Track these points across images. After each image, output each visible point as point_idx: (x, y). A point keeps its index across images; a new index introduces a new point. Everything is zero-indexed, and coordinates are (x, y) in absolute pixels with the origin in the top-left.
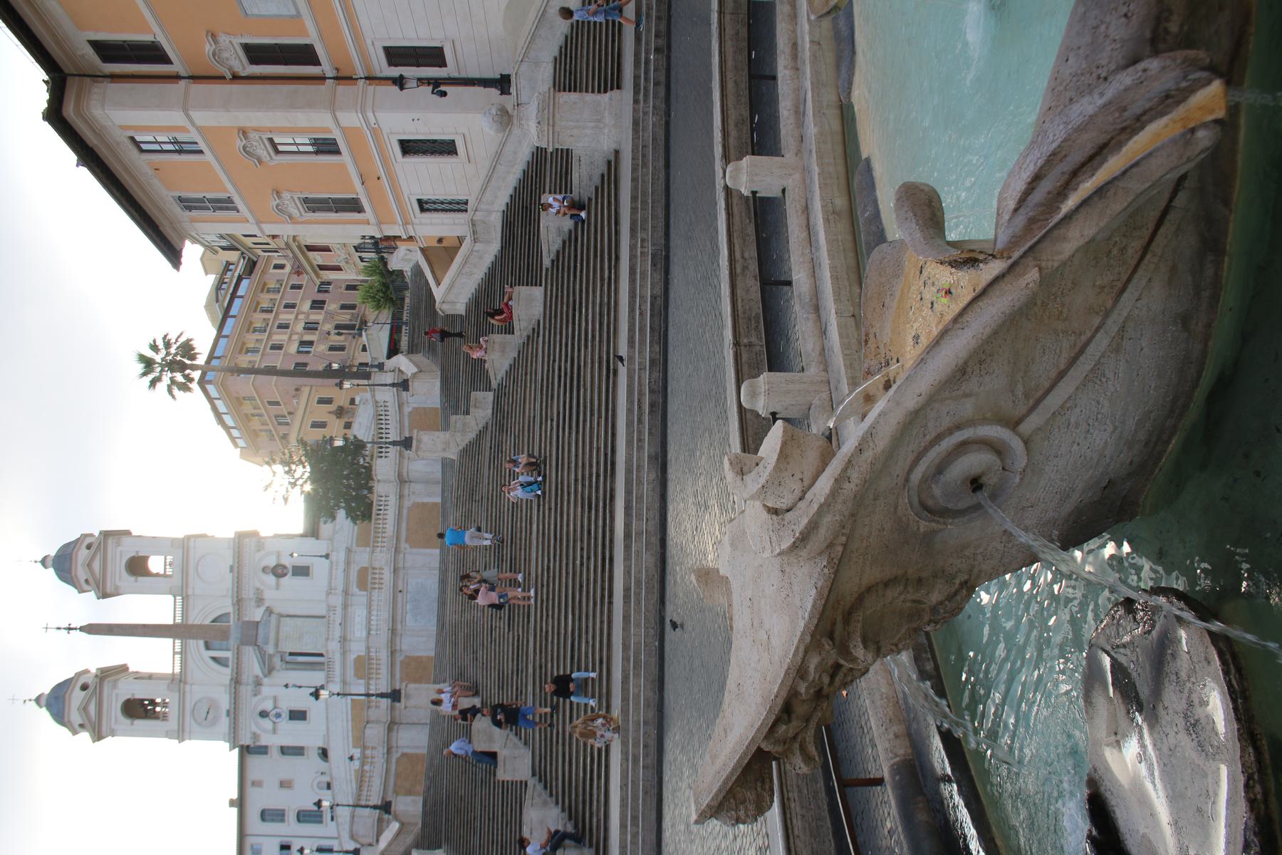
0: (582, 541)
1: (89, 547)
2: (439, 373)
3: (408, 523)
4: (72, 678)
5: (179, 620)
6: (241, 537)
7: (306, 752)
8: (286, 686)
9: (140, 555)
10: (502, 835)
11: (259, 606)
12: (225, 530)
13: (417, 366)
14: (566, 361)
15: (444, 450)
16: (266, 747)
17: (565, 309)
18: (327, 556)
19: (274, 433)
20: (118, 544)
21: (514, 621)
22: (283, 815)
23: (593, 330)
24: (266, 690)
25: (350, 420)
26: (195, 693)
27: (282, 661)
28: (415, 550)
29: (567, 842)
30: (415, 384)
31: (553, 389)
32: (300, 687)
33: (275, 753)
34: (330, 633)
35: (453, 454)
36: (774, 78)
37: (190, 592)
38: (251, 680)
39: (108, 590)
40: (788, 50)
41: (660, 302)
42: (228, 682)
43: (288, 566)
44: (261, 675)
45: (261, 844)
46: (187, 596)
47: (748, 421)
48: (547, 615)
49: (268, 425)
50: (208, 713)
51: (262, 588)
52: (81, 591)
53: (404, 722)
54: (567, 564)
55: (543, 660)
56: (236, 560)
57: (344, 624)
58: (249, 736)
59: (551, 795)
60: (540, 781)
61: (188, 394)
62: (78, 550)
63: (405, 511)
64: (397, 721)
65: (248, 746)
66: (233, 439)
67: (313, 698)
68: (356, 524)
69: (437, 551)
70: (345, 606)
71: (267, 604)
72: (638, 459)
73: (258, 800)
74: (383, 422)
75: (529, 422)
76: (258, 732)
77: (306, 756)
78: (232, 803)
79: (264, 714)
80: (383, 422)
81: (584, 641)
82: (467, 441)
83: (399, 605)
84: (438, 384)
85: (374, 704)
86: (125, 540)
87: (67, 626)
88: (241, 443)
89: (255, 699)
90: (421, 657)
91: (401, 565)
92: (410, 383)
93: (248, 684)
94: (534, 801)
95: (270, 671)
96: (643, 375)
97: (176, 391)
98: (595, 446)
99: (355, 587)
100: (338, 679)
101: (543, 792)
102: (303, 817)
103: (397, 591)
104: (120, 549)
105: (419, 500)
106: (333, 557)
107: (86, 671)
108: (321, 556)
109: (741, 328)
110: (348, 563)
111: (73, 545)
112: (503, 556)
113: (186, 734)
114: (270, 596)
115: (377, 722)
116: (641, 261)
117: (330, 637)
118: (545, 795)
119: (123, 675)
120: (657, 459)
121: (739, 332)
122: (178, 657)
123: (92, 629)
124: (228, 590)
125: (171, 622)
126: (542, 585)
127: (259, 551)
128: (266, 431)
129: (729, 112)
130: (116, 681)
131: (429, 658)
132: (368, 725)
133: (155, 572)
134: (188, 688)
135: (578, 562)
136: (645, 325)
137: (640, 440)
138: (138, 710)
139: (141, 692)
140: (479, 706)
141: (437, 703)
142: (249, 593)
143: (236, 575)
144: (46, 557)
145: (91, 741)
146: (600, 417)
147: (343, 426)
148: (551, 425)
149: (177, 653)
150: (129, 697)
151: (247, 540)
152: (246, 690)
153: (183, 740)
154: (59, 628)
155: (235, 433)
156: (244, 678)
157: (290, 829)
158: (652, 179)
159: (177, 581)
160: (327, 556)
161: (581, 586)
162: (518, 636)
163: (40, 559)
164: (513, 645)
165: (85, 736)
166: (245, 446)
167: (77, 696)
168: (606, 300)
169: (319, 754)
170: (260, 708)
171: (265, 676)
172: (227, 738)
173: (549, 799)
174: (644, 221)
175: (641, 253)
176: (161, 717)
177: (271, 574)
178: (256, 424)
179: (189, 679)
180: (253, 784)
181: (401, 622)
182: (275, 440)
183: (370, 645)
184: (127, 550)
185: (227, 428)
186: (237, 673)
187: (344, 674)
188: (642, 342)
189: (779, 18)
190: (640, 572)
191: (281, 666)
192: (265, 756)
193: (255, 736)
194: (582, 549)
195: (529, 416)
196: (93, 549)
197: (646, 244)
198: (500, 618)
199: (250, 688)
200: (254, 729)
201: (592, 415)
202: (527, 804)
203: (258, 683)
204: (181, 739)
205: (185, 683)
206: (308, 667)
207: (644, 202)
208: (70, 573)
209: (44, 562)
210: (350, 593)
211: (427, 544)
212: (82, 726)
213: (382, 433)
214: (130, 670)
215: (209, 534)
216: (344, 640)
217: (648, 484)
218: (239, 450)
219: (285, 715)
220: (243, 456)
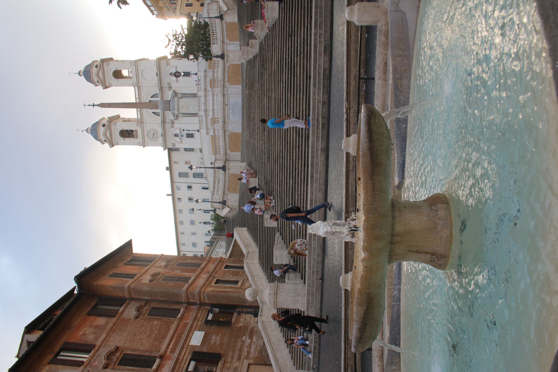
0: (296, 149)
1: (96, 67)
2: (237, 10)
3: (228, 73)
4: (98, 122)
5: (138, 101)
6: (159, 60)
7: (195, 150)
8: (183, 130)
9: (118, 69)
10: (268, 241)
11: (170, 90)
12: (153, 56)
13: (227, 6)
14: (288, 58)
15: (239, 60)
16: (179, 148)
17: (288, 30)
18: (196, 74)
19: (169, 7)
20: (108, 65)
21: (270, 160)
22: (188, 175)
23: (300, 50)
24: (176, 125)
25: (203, 2)
26: (148, 127)
28: (232, 86)
29: (290, 270)
30: (226, 17)
31: (283, 68)
32: (189, 131)
33: (182, 151)
34: (200, 107)
35: (244, 61)
36: (373, 79)
37: (141, 85)
38: (170, 121)
39: (107, 85)
40: (381, 67)
41: (327, 72)
42: (160, 122)
44: (173, 118)
45: (180, 186)
46: (140, 87)
47: (349, 255)
48: (282, 172)
49: (166, 4)
50: (154, 135)
51: (170, 82)
52: (96, 86)
53: (231, 160)
54: (290, 155)
55: (281, 189)
56: (158, 70)
57: (205, 104)
58: (171, 144)
59: (285, 244)
60: (281, 235)
61: (127, 6)
62: (92, 68)
63: (227, 68)
64: (228, 159)
65: (171, 148)
66: (152, 11)
67: (190, 169)
68: (207, 62)
69: (240, 86)
70: (205, 96)
71: (173, 89)
72: (317, 146)
73: (177, 169)
74: (214, 27)
75: (274, 71)
76: (175, 143)
77: (195, 152)
78: (167, 169)
79: (176, 135)
80: (214, 27)
81: (296, 194)
82: (249, 58)
83: (226, 110)
84: (237, 17)
85: (218, 152)
86: (111, 63)
87: (92, 104)
88: (155, 12)
89: (172, 129)
90: (237, 133)
91: (226, 93)
92: (224, 17)
93: (169, 123)
94: (278, 246)
95: (177, 117)
96: (319, 106)
97: (121, 5)
98: (301, 109)
99: (209, 87)
100: (204, 127)
101: (282, 241)
102: (196, 175)
103: (225, 105)
104: (109, 67)
105: (233, 63)
106: (199, 74)
107: (104, 118)
108: (193, 74)
109: (350, 202)
110: (205, 77)
111: (90, 66)
112: (265, 127)
113: (146, 144)
114: (174, 85)
115: (220, 160)
116: (319, 46)
117: (200, 109)
118: (282, 242)
119: (119, 119)
120: (324, 150)
121: (349, 204)
122: (139, 112)
123: (103, 105)
124: (156, 83)
125: (135, 101)
126: (280, 157)
127: (168, 66)
128: (166, 7)
129: (351, 70)
130: (116, 123)
131: (240, 133)
132: (216, 161)
133: (125, 76)
134: (144, 125)
135: (294, 157)
136: (321, 80)
137: (317, 137)
138: (127, 134)
139: (127, 127)
140: (257, 186)
141: (240, 179)
142: (165, 85)
143: (159, 77)
144: (80, 72)
145: (109, 147)
146: (303, 95)
147: (200, 5)
148: (283, 85)
149: (138, 111)
151: (162, 61)
152: (168, 126)
153: (145, 146)
154: (90, 105)
155: (152, 8)
156: (167, 121)
157: (191, 180)
158: (325, 4)
159: (134, 80)
160: (196, 74)
161: (296, 169)
162: (272, 167)
163: (78, 72)
164: (270, 169)
165: (106, 145)
166: (157, 14)
167: (102, 130)
168: (306, 38)
170: (175, 133)
171: (175, 120)
172: (162, 145)
173: (284, 245)
174: (321, 23)
175: (319, 41)
176: (135, 136)
178: (161, 3)
179: (144, 122)
180: (175, 162)
181: (228, 118)
182: (170, 11)
183: (215, 128)
184: (112, 67)
185: (148, 7)
186: (164, 119)
187: (207, 125)
188: (319, 89)
189: (378, 43)
190: (317, 197)
191: (182, 115)
193: (174, 144)
194: (296, 152)
195: (274, 68)
196: (98, 67)
197: (321, 37)
198: (264, 155)
199: (169, 125)
200: (173, 141)
201: (300, 92)
202: (275, 247)
203: (173, 123)
204: (144, 146)
205: (143, 123)
206: (193, 115)
207: (321, 13)
208: (91, 79)
209: (79, 73)
210: (207, 90)
211: (237, 84)
212: (105, 141)
213: (214, 32)
214: (121, 117)
215: (146, 58)
216: (206, 110)
217: (321, 162)
218: (155, 16)
219: (185, 136)
220: (157, 17)
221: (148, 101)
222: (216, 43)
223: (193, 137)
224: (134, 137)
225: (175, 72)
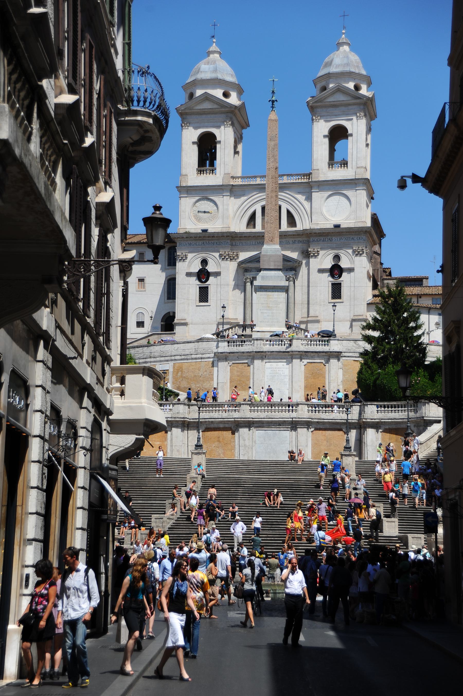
8: (224, 307)
16: (175, 265)
27: (253, 278)
43: (341, 279)
50: (205, 212)
76: (188, 260)
79: (204, 262)
90: (234, 442)
133: (336, 147)
150: (218, 139)
153: (179, 191)
154: (273, 92)
169: (169, 313)
176: (202, 169)
177: (333, 264)
192: (167, 264)
214: (244, 131)
221: (280, 203)
222: (378, 411)
223: (200, 301)
224: (199, 166)
225: (342, 267)
